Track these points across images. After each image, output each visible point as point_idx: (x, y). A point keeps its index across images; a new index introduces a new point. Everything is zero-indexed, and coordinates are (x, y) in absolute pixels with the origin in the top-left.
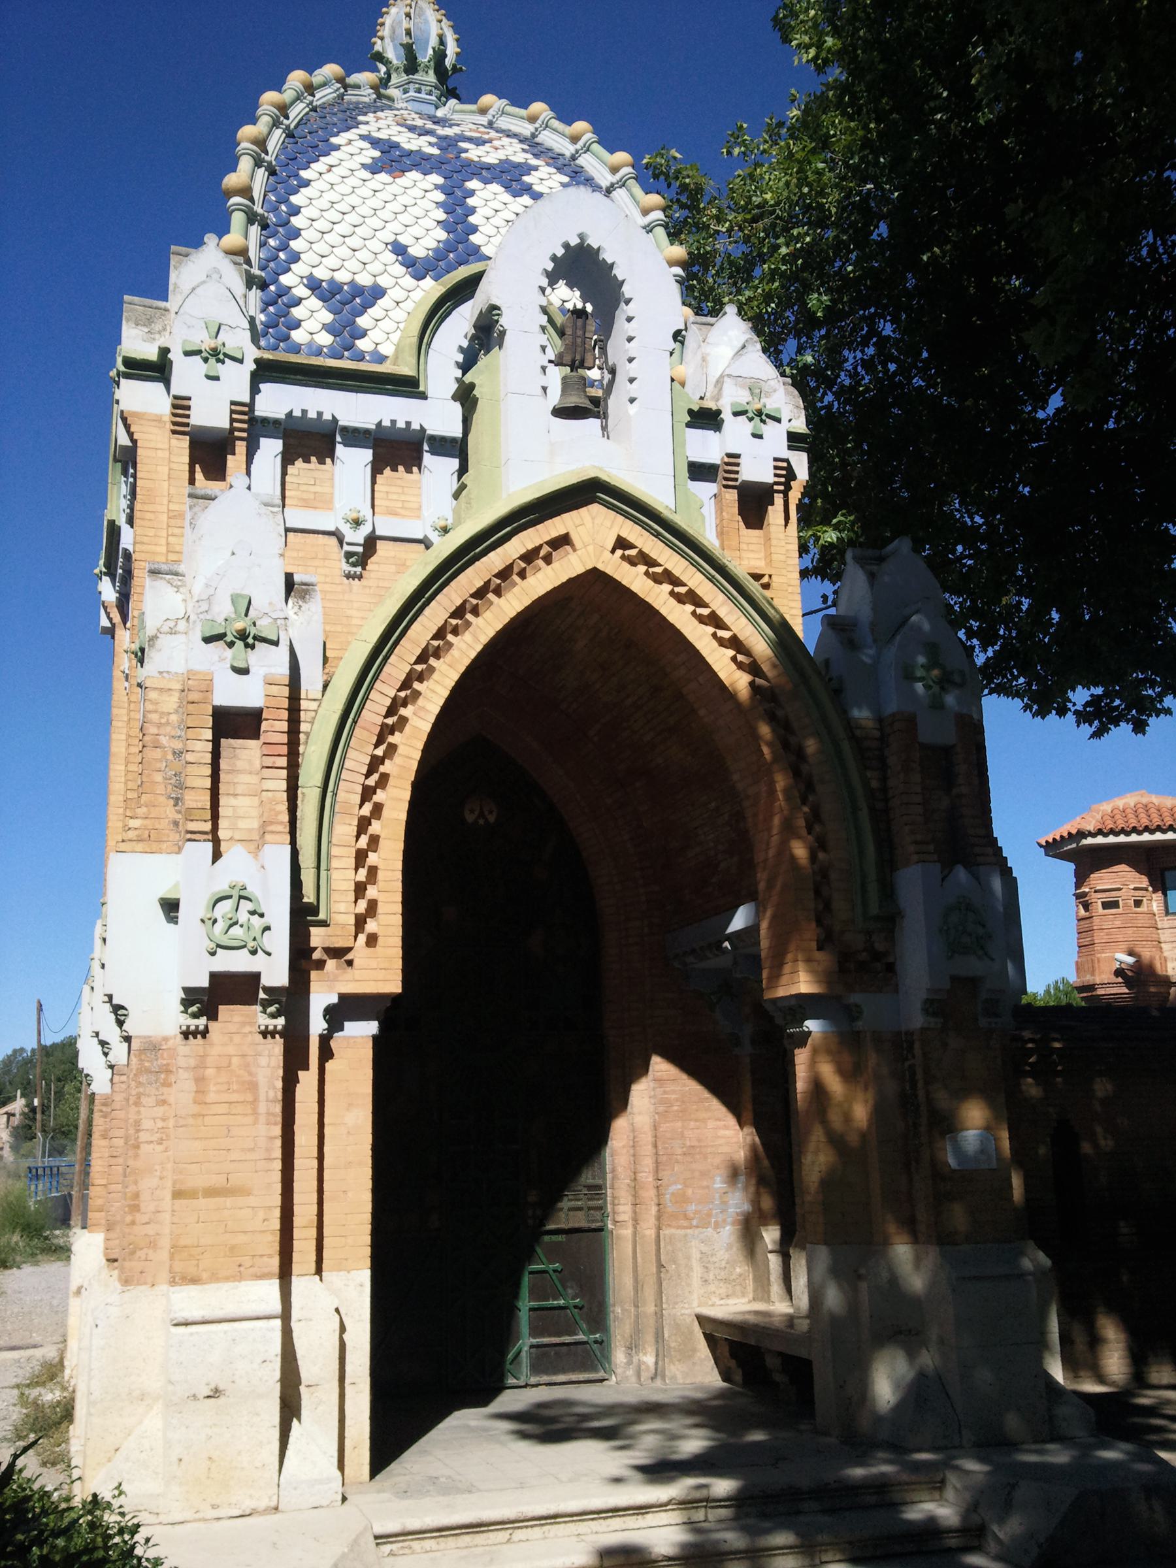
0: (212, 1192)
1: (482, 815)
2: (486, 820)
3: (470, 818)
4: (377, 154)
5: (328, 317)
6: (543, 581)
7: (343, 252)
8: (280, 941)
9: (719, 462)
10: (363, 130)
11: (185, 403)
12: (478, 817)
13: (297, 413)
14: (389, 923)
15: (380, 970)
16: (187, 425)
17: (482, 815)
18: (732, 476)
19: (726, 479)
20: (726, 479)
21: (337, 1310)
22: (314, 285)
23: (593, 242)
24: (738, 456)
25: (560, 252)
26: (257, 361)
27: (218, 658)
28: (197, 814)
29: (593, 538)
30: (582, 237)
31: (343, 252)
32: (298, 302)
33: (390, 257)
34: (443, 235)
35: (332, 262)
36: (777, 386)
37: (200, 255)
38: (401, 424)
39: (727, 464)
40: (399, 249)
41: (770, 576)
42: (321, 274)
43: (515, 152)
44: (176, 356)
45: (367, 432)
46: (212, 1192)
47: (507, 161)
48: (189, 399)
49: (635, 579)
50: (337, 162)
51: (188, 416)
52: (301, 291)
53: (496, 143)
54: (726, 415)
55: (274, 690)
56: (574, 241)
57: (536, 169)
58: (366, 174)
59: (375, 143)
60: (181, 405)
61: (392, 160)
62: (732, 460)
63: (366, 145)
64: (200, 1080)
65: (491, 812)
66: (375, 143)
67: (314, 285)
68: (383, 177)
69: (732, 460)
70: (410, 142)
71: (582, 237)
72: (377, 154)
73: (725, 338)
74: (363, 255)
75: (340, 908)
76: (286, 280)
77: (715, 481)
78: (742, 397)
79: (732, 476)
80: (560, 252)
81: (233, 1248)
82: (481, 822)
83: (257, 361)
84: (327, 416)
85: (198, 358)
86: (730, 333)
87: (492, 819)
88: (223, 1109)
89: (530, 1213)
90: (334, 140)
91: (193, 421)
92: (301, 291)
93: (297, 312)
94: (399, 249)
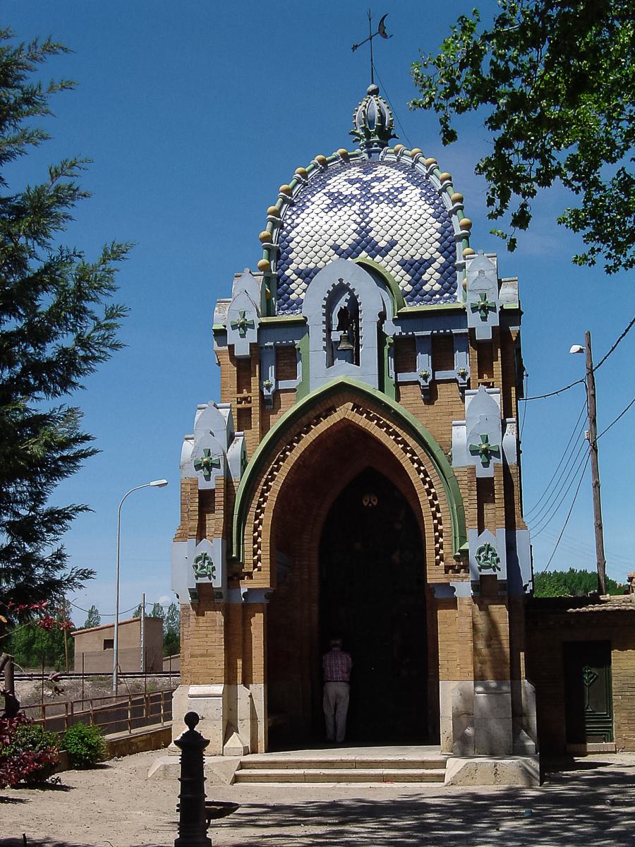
0: (202, 655)
1: (370, 502)
2: (373, 505)
3: (365, 504)
7: (312, 254)
8: (218, 573)
12: (369, 503)
14: (265, 563)
15: (260, 580)
17: (370, 502)
21: (251, 696)
22: (299, 273)
23: (345, 282)
26: (259, 324)
27: (202, 473)
30: (341, 280)
31: (312, 254)
32: (293, 281)
33: (332, 251)
34: (355, 236)
35: (307, 260)
40: (336, 248)
41: (493, 383)
42: (302, 266)
44: (229, 329)
46: (202, 655)
49: (361, 421)
54: (468, 311)
55: (219, 482)
56: (337, 283)
57: (406, 188)
59: (330, 195)
60: (231, 348)
61: (338, 200)
65: (374, 500)
66: (330, 195)
71: (341, 280)
74: (321, 254)
75: (248, 558)
76: (288, 273)
81: (209, 674)
82: (370, 505)
83: (259, 324)
87: (375, 503)
88: (205, 628)
92: (294, 277)
93: (293, 286)
94: (336, 248)
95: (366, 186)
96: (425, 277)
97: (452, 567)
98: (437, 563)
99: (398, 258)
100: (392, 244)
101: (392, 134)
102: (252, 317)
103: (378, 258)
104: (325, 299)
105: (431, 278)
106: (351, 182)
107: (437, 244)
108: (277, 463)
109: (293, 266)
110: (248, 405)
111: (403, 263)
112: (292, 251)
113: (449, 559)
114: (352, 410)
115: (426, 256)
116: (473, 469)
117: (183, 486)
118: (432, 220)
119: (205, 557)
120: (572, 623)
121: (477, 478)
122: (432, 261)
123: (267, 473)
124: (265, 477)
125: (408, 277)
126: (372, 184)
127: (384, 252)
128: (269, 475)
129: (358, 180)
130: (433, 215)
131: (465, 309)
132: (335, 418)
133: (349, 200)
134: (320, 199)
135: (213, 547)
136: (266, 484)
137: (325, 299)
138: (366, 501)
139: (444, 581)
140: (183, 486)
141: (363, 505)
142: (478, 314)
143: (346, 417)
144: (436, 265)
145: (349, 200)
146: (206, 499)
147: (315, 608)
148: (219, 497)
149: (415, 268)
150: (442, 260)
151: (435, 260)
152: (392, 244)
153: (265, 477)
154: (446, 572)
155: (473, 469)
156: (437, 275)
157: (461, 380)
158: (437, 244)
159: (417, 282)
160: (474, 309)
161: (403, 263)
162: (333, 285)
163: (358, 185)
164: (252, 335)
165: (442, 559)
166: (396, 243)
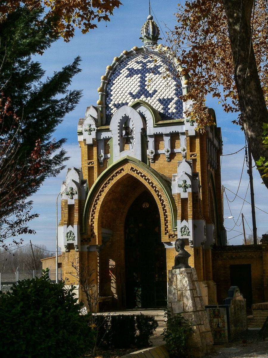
1: (146, 206)
3: (144, 207)
6: (119, 177)
12: (145, 206)
17: (146, 206)
19: (187, 135)
20: (187, 135)
22: (115, 105)
25: (121, 118)
28: (66, 221)
29: (127, 169)
30: (125, 114)
32: (112, 109)
33: (129, 96)
39: (186, 132)
40: (131, 94)
41: (196, 154)
42: (116, 103)
49: (134, 174)
52: (112, 107)
54: (185, 122)
56: (124, 116)
57: (161, 66)
58: (125, 78)
59: (128, 69)
62: (187, 131)
64: (68, 258)
65: (147, 205)
66: (128, 69)
68: (129, 78)
69: (187, 131)
71: (125, 114)
76: (110, 105)
80: (121, 118)
87: (148, 206)
89: (156, 278)
92: (112, 107)
94: (131, 94)
95: (144, 65)
96: (169, 106)
97: (172, 235)
98: (166, 234)
99: (157, 98)
100: (155, 91)
102: (94, 126)
103: (149, 98)
104: (119, 123)
105: (172, 108)
106: (138, 63)
108: (100, 192)
109: (112, 103)
110: (92, 165)
111: (160, 100)
112: (112, 95)
113: (170, 232)
114: (131, 170)
116: (179, 195)
117: (62, 203)
119: (71, 232)
120: (234, 257)
121: (181, 198)
122: (173, 99)
123: (96, 197)
124: (95, 198)
125: (162, 107)
126: (147, 64)
127: (151, 96)
128: (97, 198)
129: (141, 62)
131: (184, 122)
132: (124, 173)
133: (137, 72)
134: (124, 72)
135: (75, 229)
136: (96, 201)
137: (119, 123)
138: (144, 205)
139: (168, 241)
140: (62, 203)
141: (142, 207)
142: (189, 124)
143: (128, 173)
144: (174, 101)
145: (137, 72)
146: (71, 208)
147: (123, 252)
148: (76, 207)
149: (165, 102)
151: (173, 99)
152: (155, 91)
153: (95, 198)
154: (169, 237)
155: (179, 195)
156: (175, 106)
157: (183, 153)
158: (174, 92)
159: (166, 108)
160: (188, 121)
161: (160, 100)
162: (122, 117)
163: (141, 64)
164: (94, 133)
165: (167, 232)
166: (156, 91)
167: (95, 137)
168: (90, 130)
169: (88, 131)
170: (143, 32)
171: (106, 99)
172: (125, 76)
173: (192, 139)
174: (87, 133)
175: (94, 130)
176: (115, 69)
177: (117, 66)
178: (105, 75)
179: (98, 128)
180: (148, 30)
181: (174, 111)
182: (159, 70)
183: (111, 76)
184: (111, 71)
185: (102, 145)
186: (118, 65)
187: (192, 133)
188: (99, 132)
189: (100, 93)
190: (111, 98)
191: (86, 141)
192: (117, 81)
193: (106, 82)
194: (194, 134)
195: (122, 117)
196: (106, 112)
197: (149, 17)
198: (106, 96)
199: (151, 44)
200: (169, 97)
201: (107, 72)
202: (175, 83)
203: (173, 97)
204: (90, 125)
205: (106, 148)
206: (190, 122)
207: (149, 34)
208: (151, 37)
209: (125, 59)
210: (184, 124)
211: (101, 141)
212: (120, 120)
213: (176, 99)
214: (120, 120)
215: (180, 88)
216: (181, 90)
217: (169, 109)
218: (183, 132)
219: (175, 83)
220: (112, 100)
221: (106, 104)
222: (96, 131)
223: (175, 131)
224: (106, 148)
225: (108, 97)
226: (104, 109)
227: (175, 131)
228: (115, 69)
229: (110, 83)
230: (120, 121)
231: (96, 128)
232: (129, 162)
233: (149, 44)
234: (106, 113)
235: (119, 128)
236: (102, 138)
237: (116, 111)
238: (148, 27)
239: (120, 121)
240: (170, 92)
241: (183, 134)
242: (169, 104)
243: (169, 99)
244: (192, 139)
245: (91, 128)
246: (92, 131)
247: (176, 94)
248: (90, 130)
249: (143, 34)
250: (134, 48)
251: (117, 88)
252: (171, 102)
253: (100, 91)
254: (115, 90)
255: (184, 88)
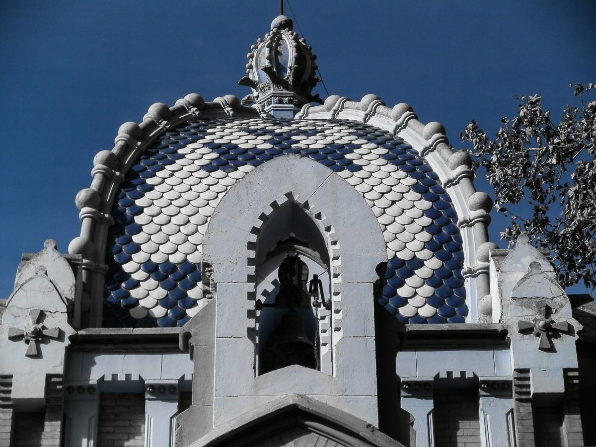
4: (215, 155)
5: (161, 292)
9: (512, 379)
10: (208, 138)
11: (8, 380)
13: (108, 378)
16: (9, 399)
18: (524, 390)
22: (151, 268)
24: (527, 371)
25: (269, 211)
30: (289, 195)
32: (137, 284)
36: (563, 302)
37: (39, 257)
38: (456, 375)
43: (340, 136)
45: (171, 387)
47: (332, 144)
48: (11, 377)
50: (382, 168)
51: (10, 392)
53: (327, 132)
54: (514, 334)
56: (282, 200)
57: (359, 147)
58: (202, 173)
63: (206, 150)
67: (151, 268)
68: (219, 173)
70: (245, 142)
71: (289, 195)
72: (215, 155)
73: (519, 265)
76: (127, 267)
77: (510, 397)
78: (531, 316)
79: (524, 390)
80: (269, 211)
83: (71, 338)
84: (135, 378)
85: (22, 343)
86: (523, 260)
90: (180, 151)
91: (13, 396)
96: (402, 292)
101: (313, 93)
102: (58, 321)
104: (254, 230)
107: (425, 236)
112: (139, 229)
115: (403, 255)
118: (413, 195)
130: (415, 187)
131: (505, 332)
134: (196, 153)
150: (433, 263)
151: (420, 264)
156: (427, 290)
158: (425, 236)
160: (526, 330)
162: (274, 205)
163: (268, 137)
164: (54, 357)
167: (60, 370)
168: (40, 337)
169: (27, 342)
170: (254, 63)
171: (110, 242)
172: (202, 167)
173: (545, 411)
174: (22, 347)
175: (61, 336)
176: (156, 142)
177: (162, 133)
178: (115, 150)
179: (82, 332)
180: (278, 53)
181: (427, 311)
182: (348, 156)
183: (136, 161)
184: (139, 143)
185: (89, 412)
186: (168, 131)
187: (548, 380)
188: (80, 350)
189: (86, 209)
190: (136, 239)
191: (10, 385)
192: (164, 179)
193: (118, 173)
194: (558, 387)
195: (274, 205)
196: (107, 294)
197: (278, 20)
198: (111, 229)
199: (290, 102)
200: (400, 256)
201: (120, 143)
202: (426, 204)
203: (420, 255)
204: (42, 316)
205: (108, 433)
206: (538, 335)
207: (281, 68)
208: (288, 75)
209: (196, 119)
210: (506, 346)
211: (87, 396)
212: (263, 217)
213: (433, 263)
214: (263, 217)
215: (447, 223)
216: (457, 232)
217: (404, 302)
218: (501, 379)
219: (426, 204)
220: (137, 248)
221: (109, 259)
222: (67, 342)
223: (463, 373)
224: (108, 433)
225: (121, 232)
226: (100, 281)
227: (463, 373)
228: (156, 142)
229: (134, 182)
230: (259, 224)
231: (69, 331)
232: (306, 431)
233: (281, 102)
234: (109, 299)
235: (252, 254)
236: (94, 379)
237: (221, 196)
238: (278, 44)
239: (259, 224)
240: (406, 236)
241: (499, 389)
242: (402, 283)
243: (403, 262)
244: (545, 411)
245: (44, 328)
246: (46, 339)
247: (433, 246)
248: (40, 337)
249: (254, 68)
250: (228, 97)
251: (164, 202)
252: (411, 274)
253: (88, 203)
254: (154, 210)
255: (468, 223)
